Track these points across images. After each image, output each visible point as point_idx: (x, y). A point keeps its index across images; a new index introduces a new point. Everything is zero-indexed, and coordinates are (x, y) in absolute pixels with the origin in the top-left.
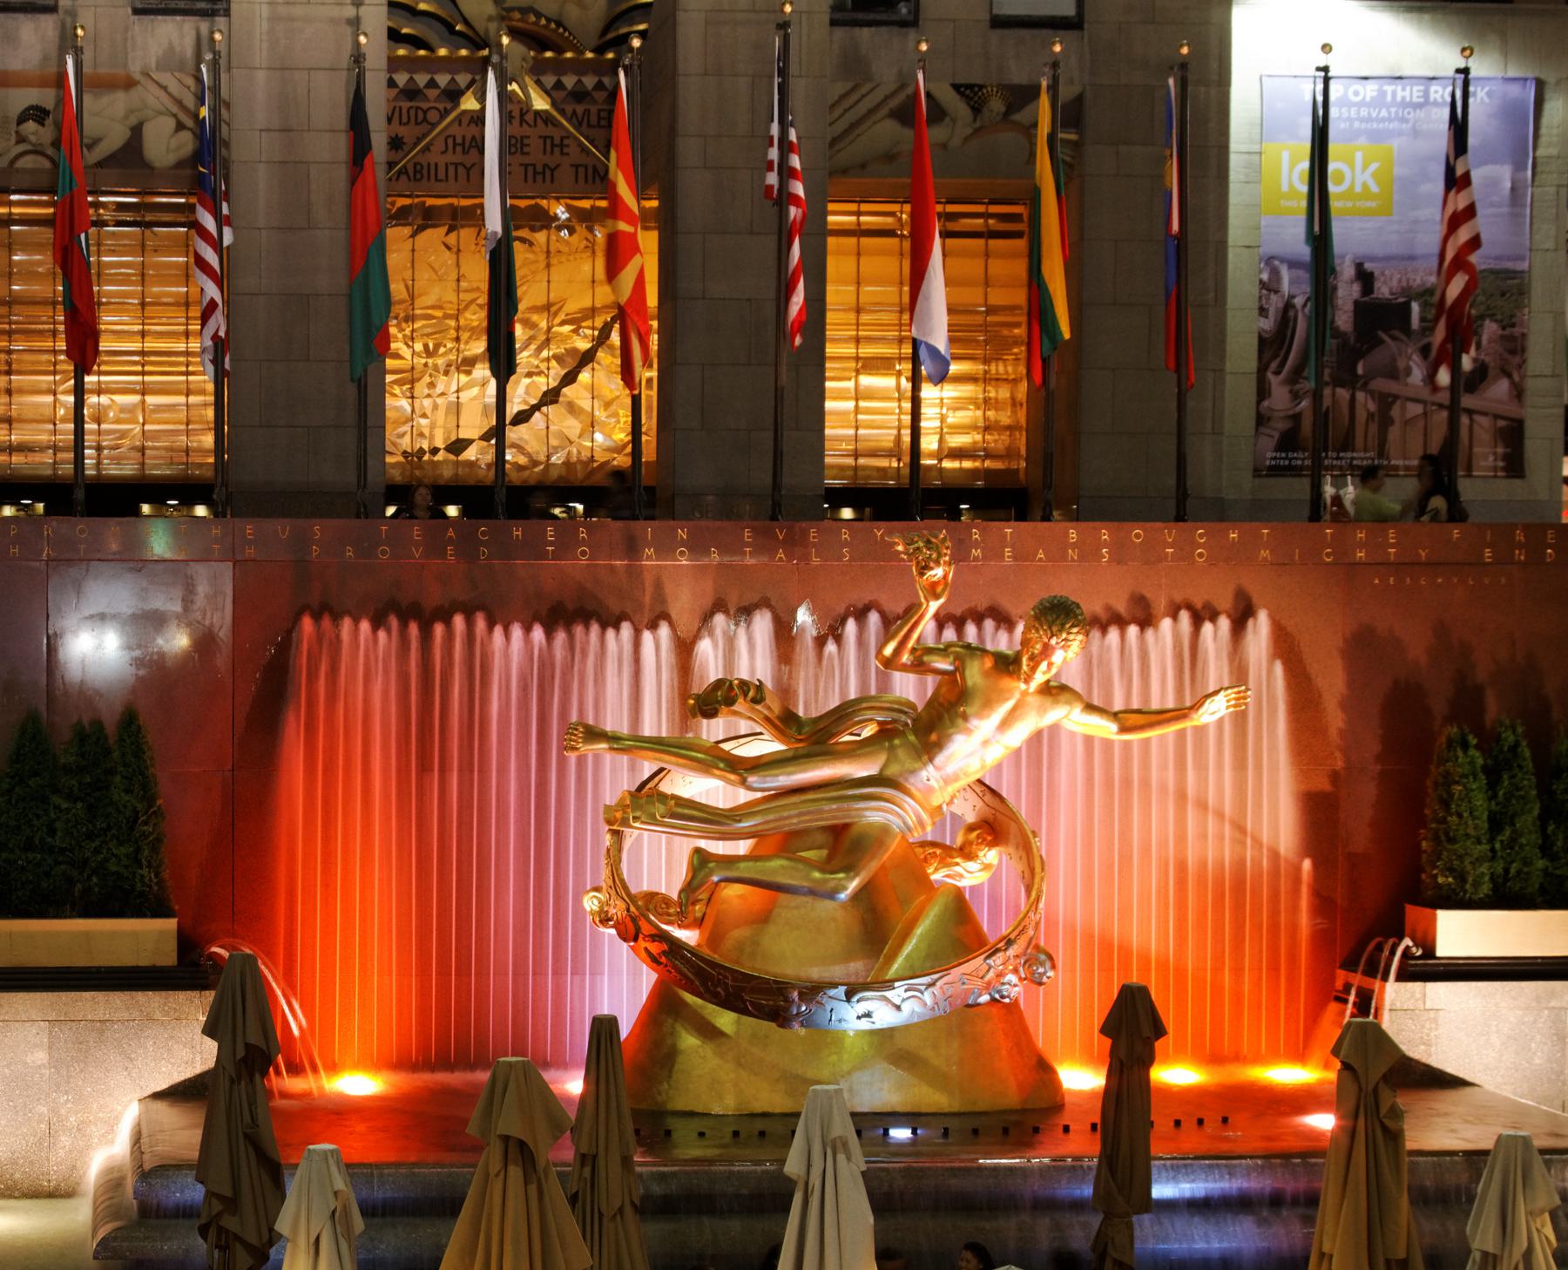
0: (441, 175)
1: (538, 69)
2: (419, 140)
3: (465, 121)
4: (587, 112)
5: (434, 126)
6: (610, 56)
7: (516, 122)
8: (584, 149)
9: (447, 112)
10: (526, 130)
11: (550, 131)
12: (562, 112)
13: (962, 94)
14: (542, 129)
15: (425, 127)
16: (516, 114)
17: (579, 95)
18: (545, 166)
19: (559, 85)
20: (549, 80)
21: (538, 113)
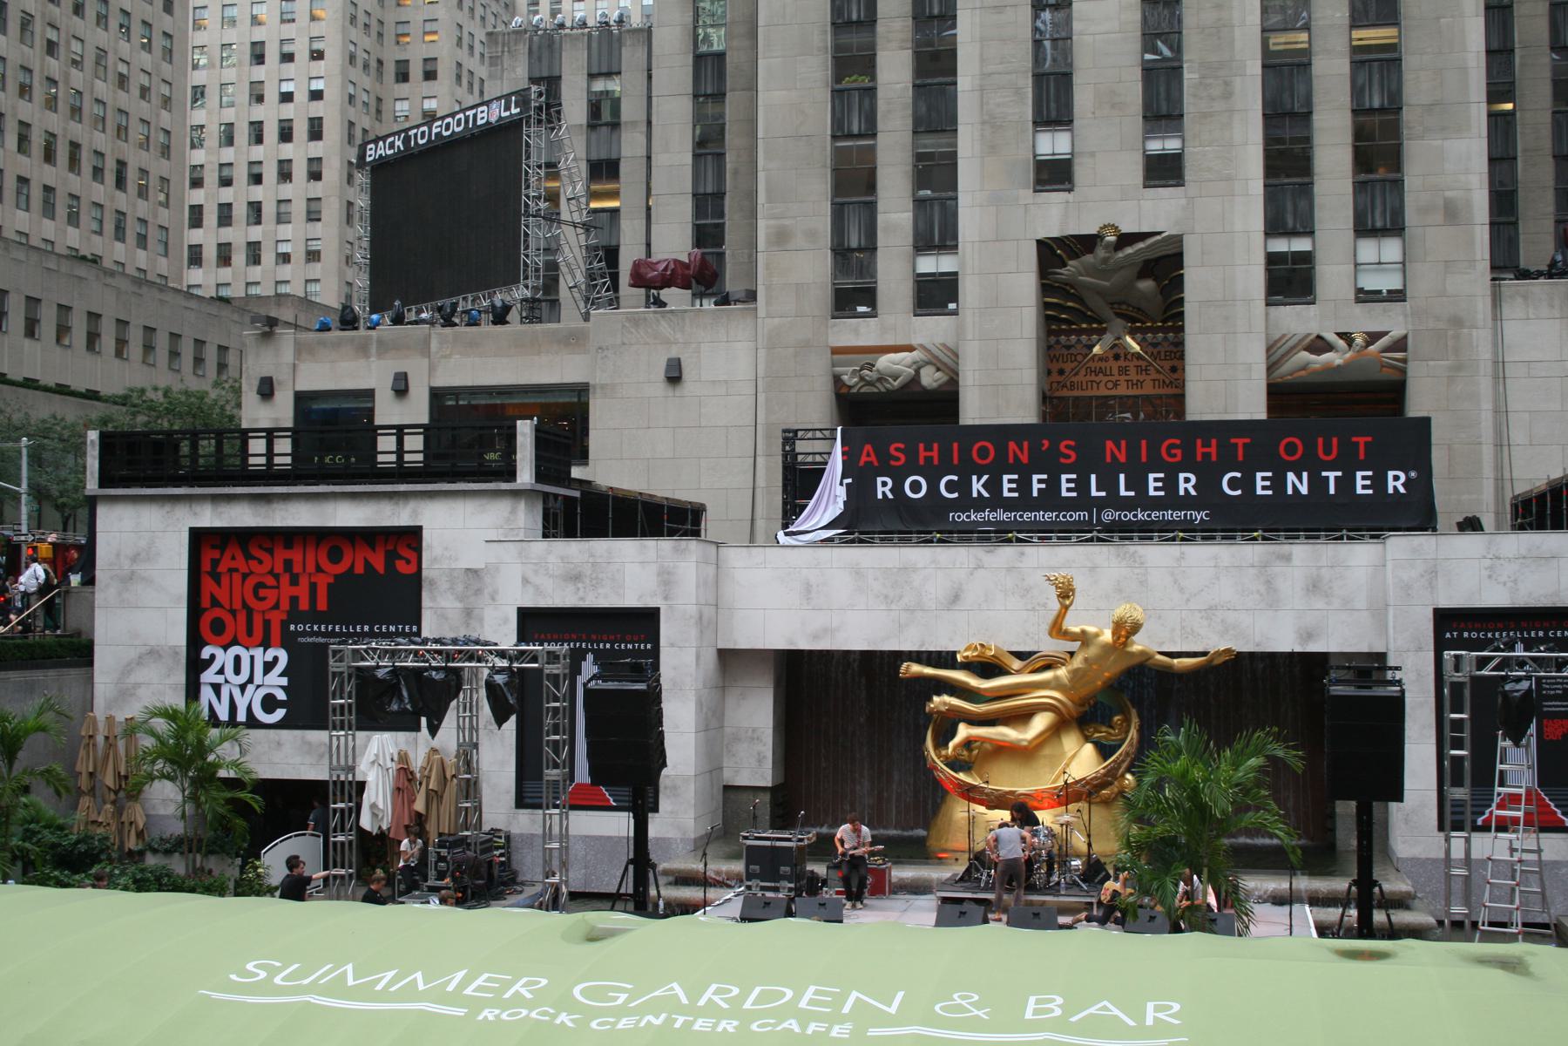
0: (1084, 387)
1: (1132, 333)
2: (1073, 370)
3: (1096, 358)
4: (1159, 352)
5: (1080, 362)
6: (1170, 324)
7: (1122, 359)
8: (1158, 372)
9: (1087, 355)
10: (1127, 363)
11: (1141, 363)
12: (1146, 353)
13: (1341, 338)
14: (1136, 362)
15: (1076, 363)
16: (1122, 355)
17: (1155, 345)
18: (1138, 381)
19: (1144, 339)
20: (1139, 336)
21: (1133, 354)
